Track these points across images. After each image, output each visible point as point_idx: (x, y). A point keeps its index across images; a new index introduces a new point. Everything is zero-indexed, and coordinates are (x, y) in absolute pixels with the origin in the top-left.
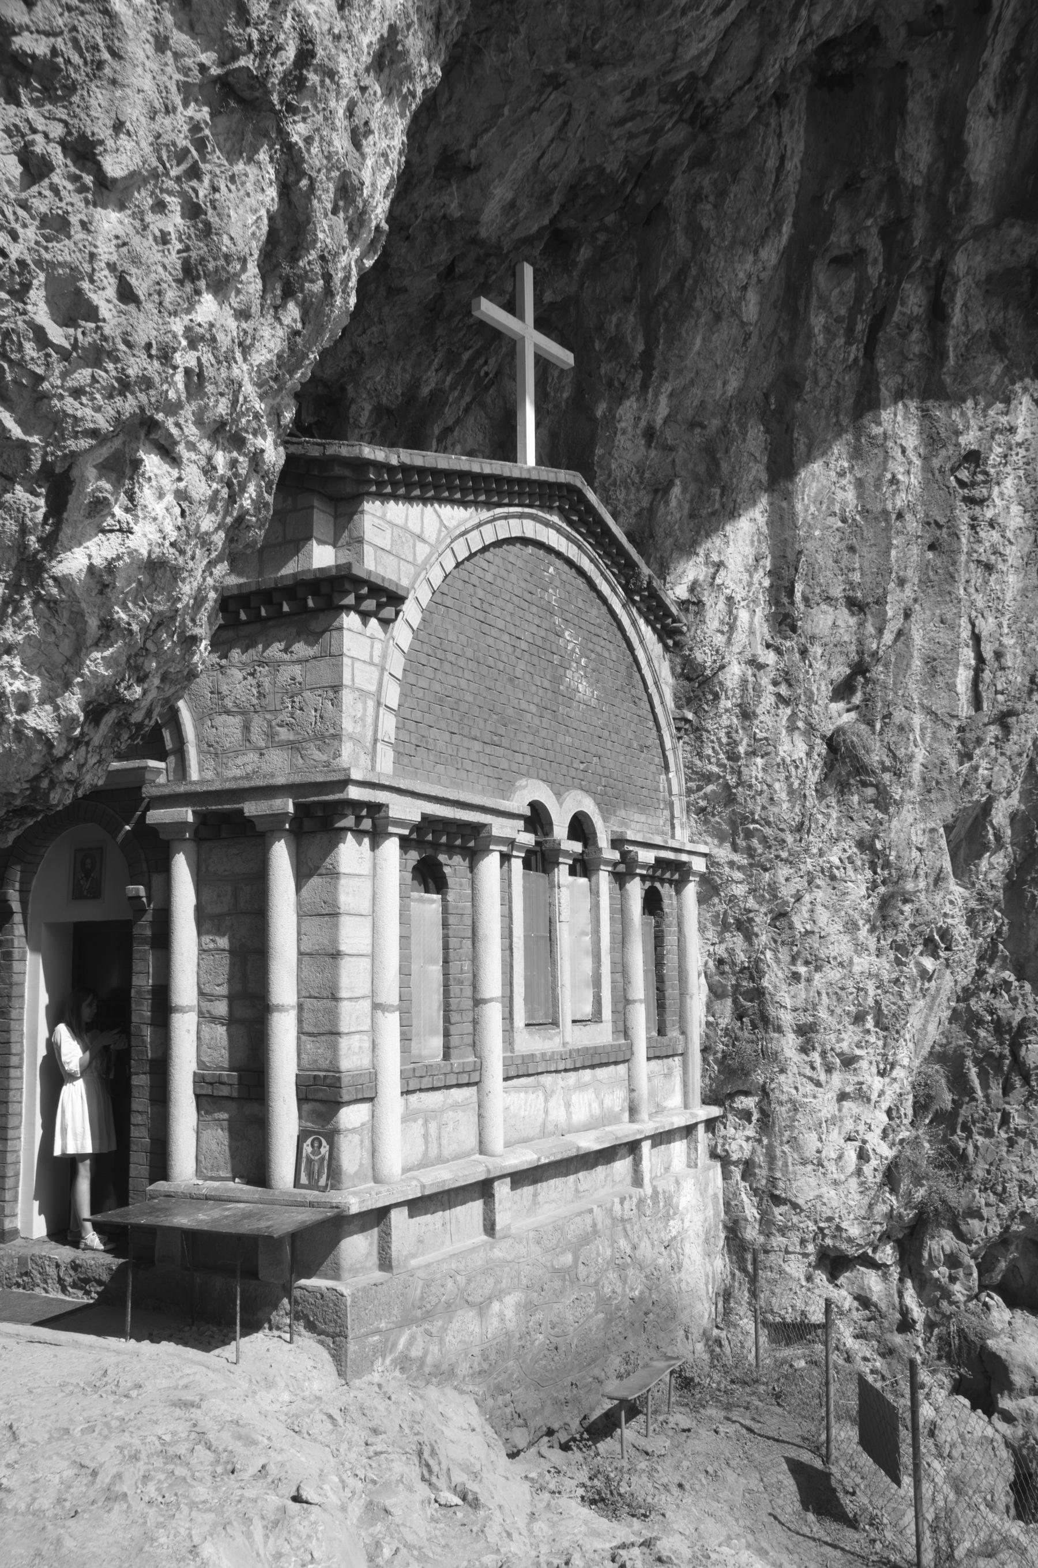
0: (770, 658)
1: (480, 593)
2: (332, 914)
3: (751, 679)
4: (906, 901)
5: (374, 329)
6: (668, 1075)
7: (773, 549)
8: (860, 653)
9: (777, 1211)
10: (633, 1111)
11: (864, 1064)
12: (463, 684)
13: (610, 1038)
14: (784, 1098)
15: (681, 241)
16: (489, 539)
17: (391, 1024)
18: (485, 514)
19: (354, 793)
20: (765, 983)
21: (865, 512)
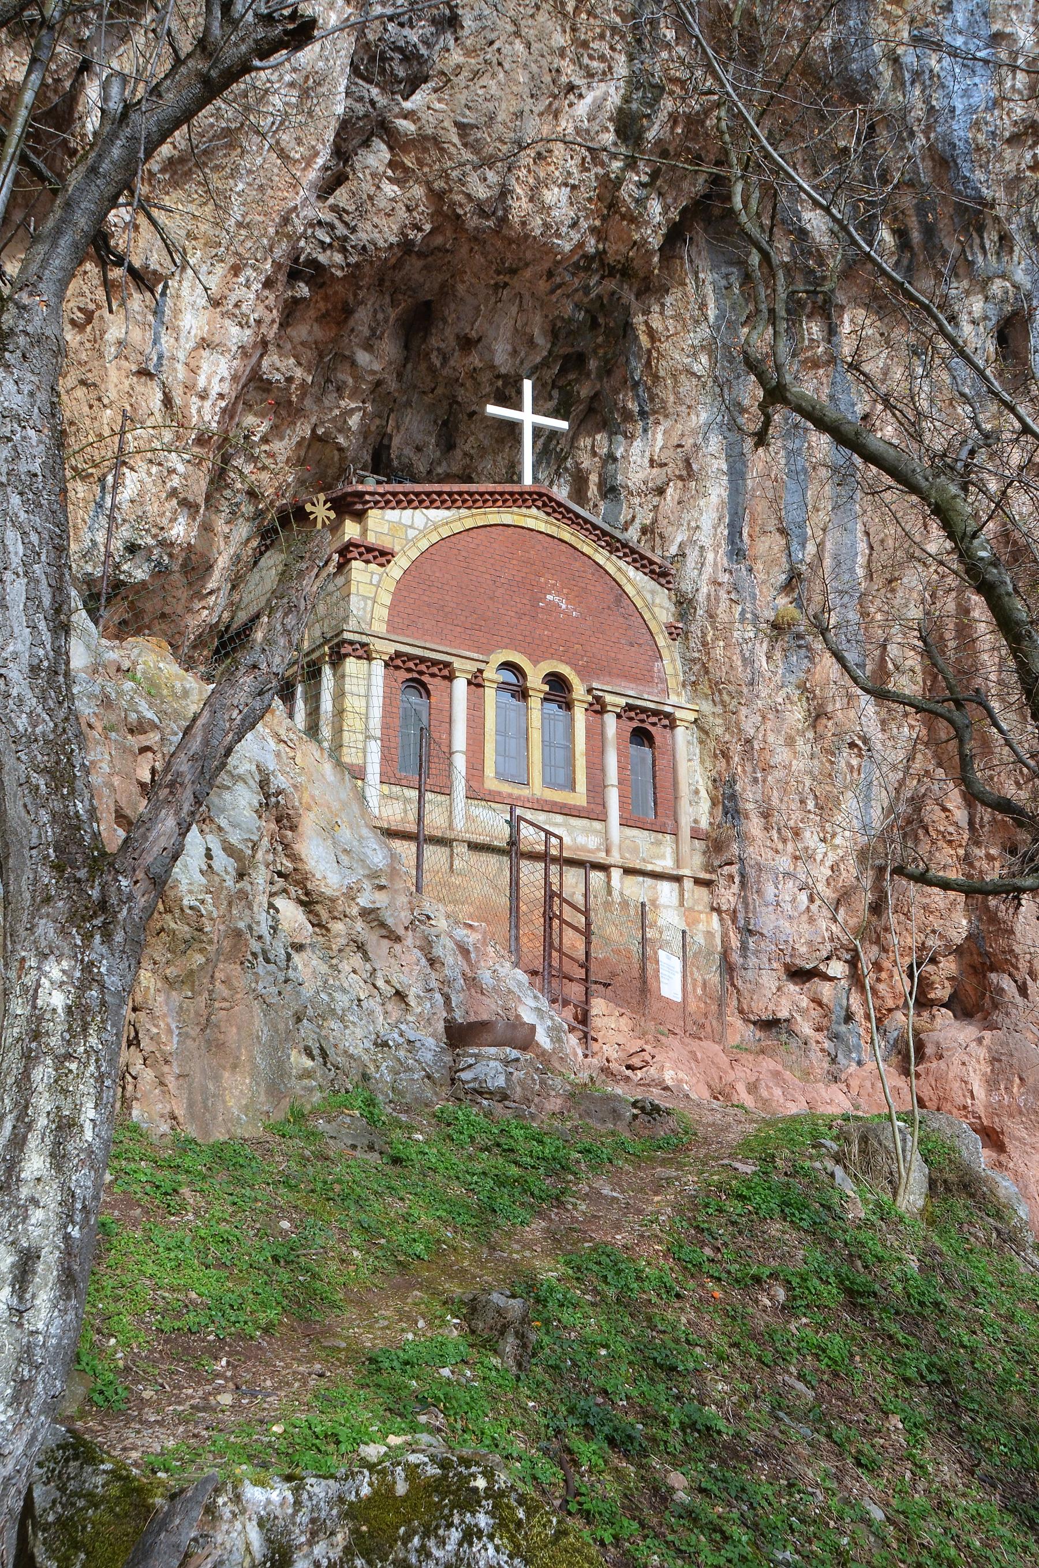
0: (725, 578)
1: (464, 553)
3: (713, 593)
4: (829, 719)
7: (729, 510)
9: (750, 940)
11: (808, 834)
12: (447, 598)
13: (585, 804)
14: (752, 862)
15: (644, 340)
17: (374, 749)
18: (464, 512)
19: (347, 636)
20: (737, 787)
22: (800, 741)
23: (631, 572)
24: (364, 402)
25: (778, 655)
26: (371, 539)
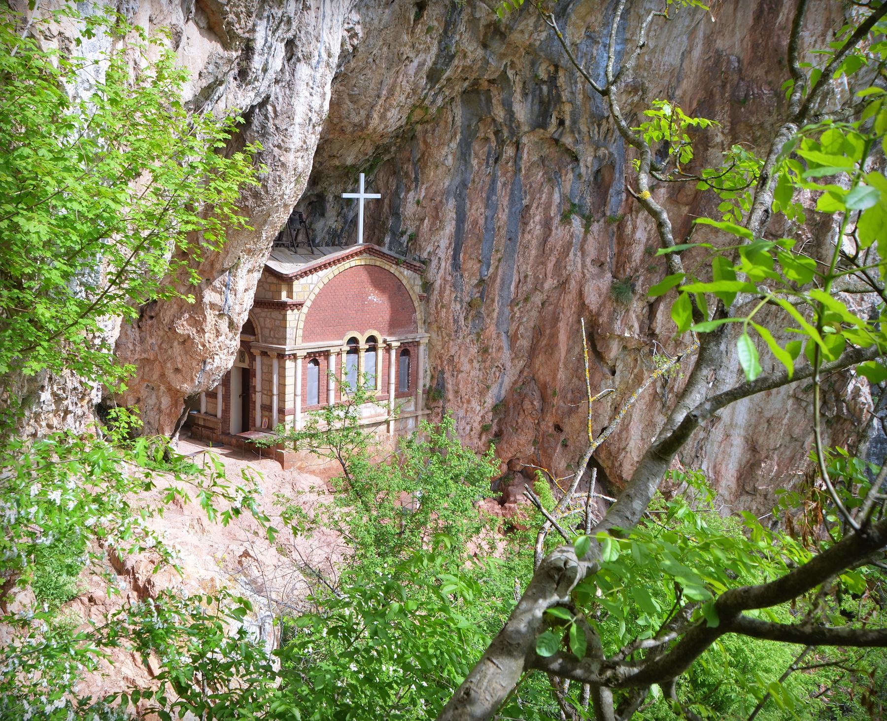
0: (449, 278)
2: (285, 377)
6: (409, 401)
8: (481, 276)
10: (389, 413)
16: (336, 272)
21: (486, 229)
22: (475, 362)
23: (406, 272)
25: (470, 318)
26: (296, 298)
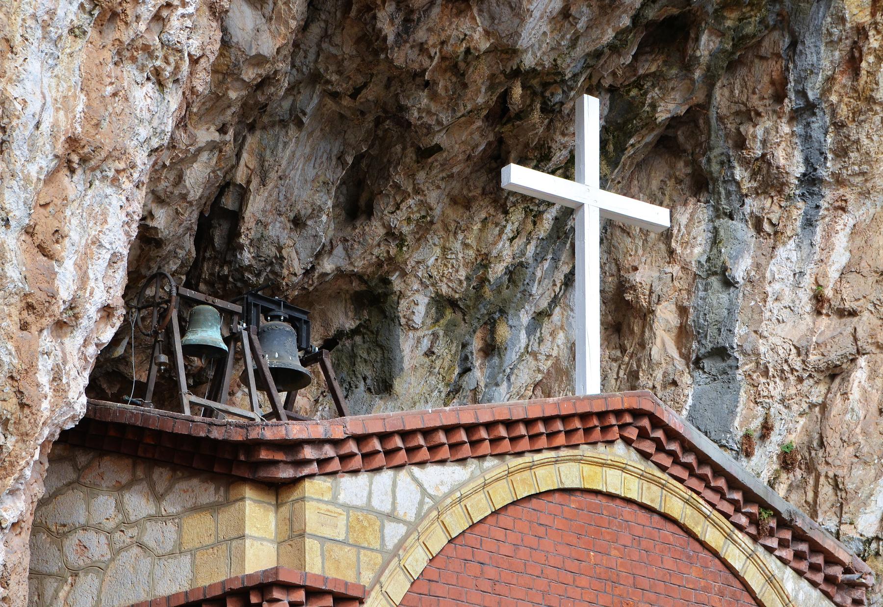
1: (491, 572)
5: (411, 202)
16: (502, 497)
24: (222, 130)
